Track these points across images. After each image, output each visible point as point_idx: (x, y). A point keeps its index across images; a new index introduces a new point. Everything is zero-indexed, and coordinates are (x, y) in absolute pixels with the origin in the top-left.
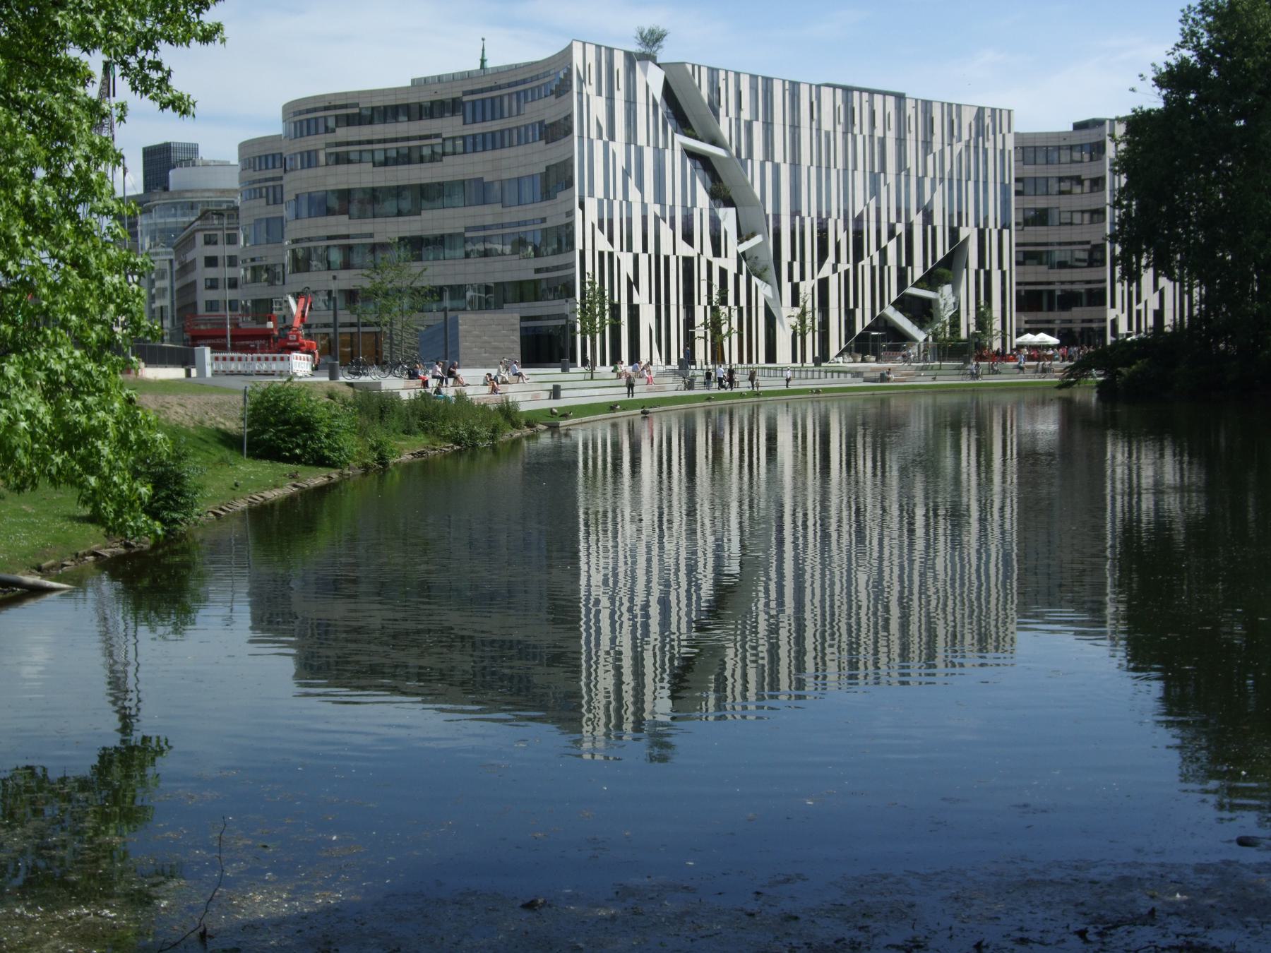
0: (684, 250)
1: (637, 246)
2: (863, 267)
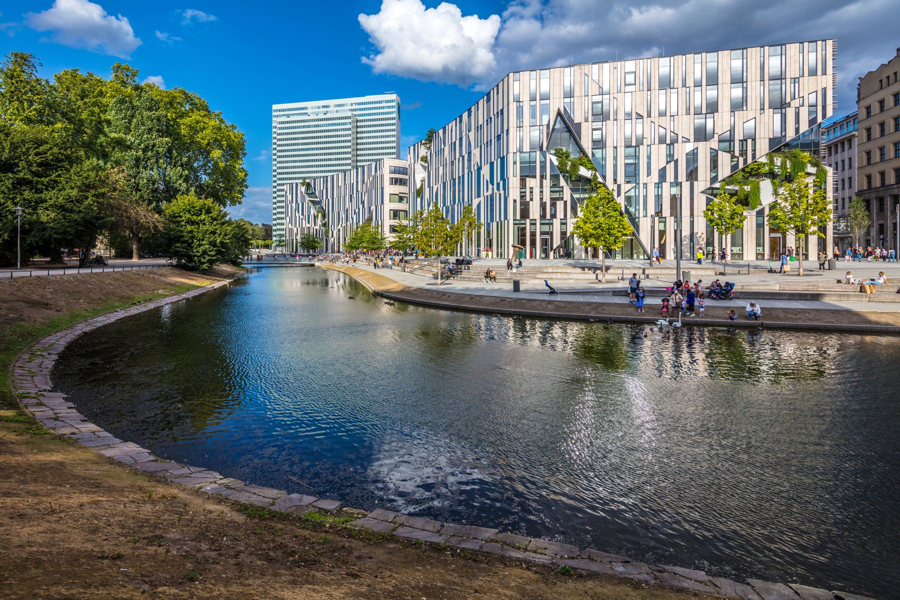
0: (308, 225)
1: (298, 226)
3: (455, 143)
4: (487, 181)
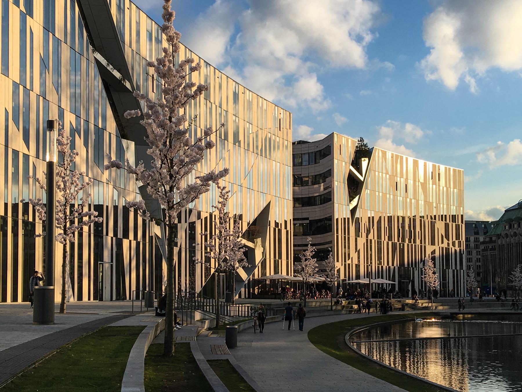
2: (215, 216)
4: (442, 236)
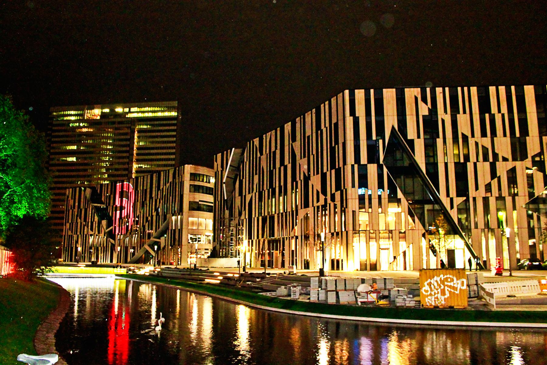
3: (275, 153)
4: (318, 192)
